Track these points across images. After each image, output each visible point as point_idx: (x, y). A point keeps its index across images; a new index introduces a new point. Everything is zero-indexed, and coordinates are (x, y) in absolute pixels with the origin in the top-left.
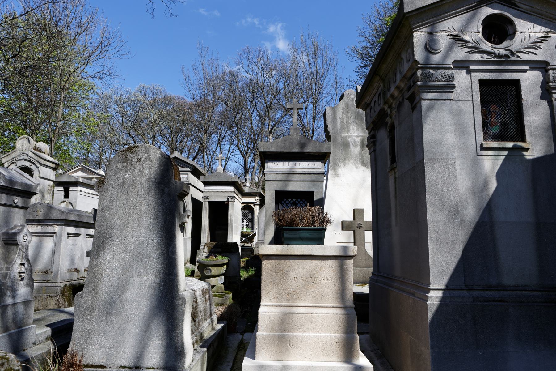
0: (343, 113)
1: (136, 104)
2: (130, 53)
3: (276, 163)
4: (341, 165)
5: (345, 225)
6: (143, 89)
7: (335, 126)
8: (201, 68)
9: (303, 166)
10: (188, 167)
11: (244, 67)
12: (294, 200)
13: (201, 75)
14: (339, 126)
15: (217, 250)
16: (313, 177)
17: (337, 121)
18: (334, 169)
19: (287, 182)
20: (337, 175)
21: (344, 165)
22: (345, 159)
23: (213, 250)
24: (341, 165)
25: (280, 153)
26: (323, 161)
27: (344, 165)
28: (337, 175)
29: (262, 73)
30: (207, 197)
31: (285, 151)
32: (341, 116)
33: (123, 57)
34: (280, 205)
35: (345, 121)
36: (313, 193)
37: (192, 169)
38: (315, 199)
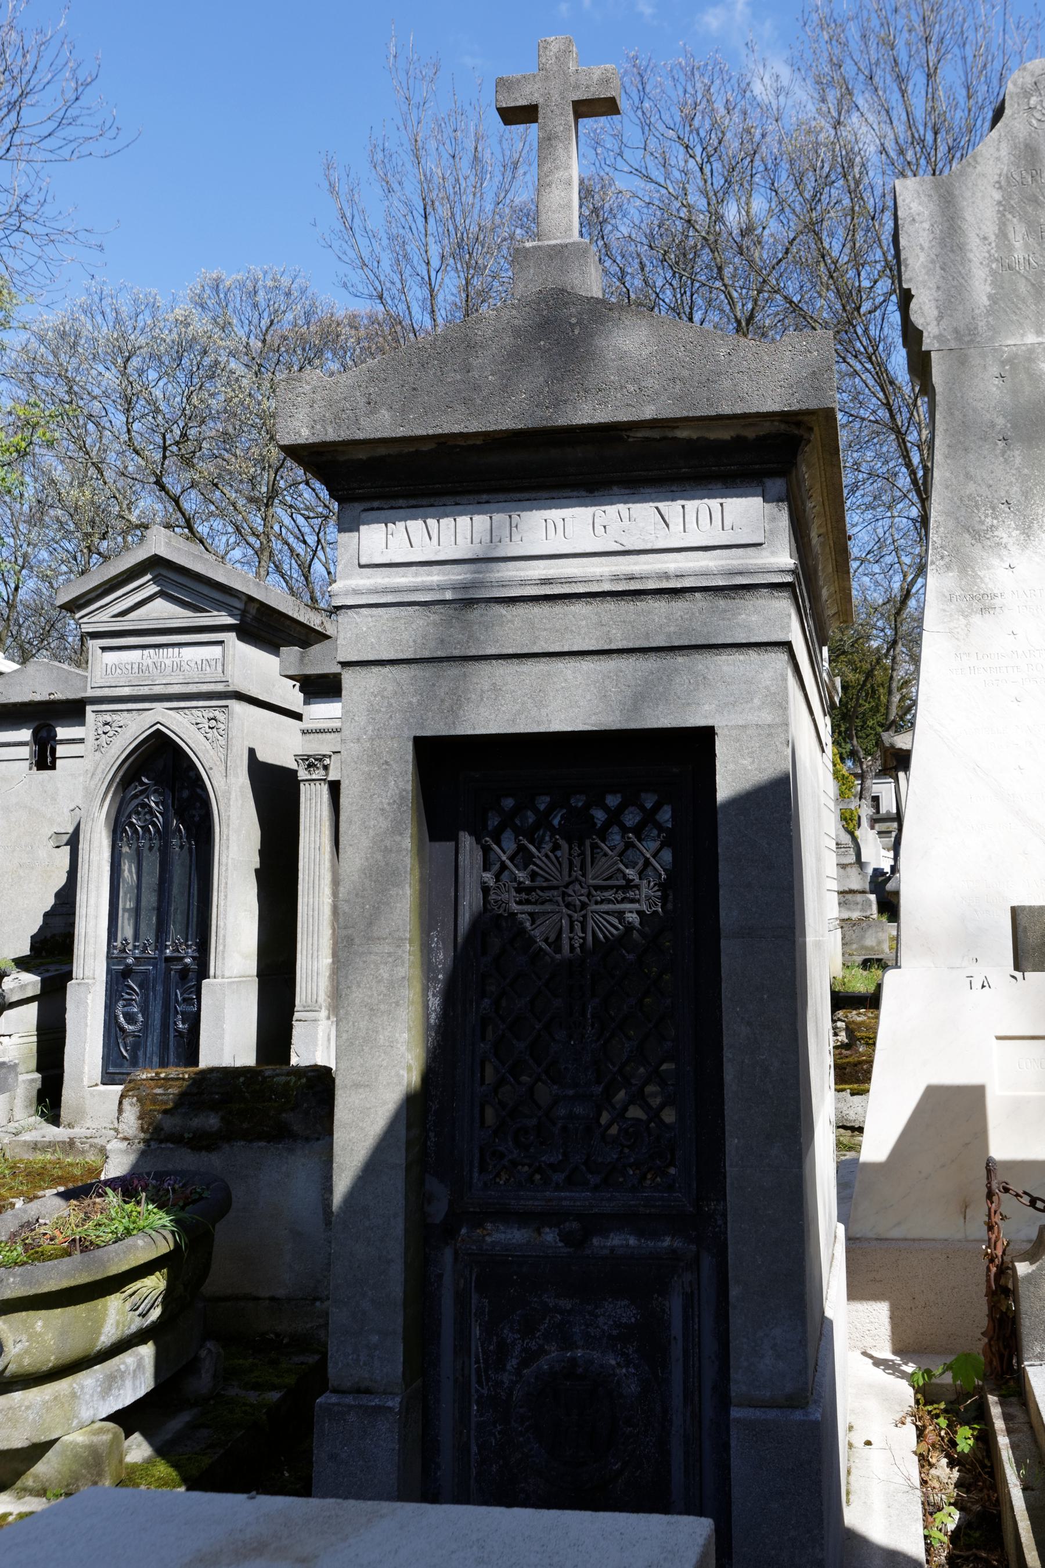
0: (1005, 208)
1: (187, 355)
2: (113, 132)
3: (416, 526)
4: (1007, 533)
5: (1032, 938)
6: (217, 289)
7: (954, 293)
8: (408, 159)
9: (568, 537)
10: (220, 606)
11: (627, 154)
12: (578, 801)
13: (412, 191)
14: (981, 288)
15: (196, 1122)
16: (661, 620)
17: (965, 261)
18: (963, 564)
19: (453, 671)
20: (983, 603)
21: (1027, 531)
22: (1026, 494)
23: (170, 1124)
24: (1007, 533)
25: (444, 443)
26: (777, 485)
27: (1027, 531)
28: (983, 603)
29: (707, 169)
30: (321, 758)
31: (474, 426)
32: (990, 229)
33: (85, 149)
34: (467, 841)
35: (1019, 254)
36: (700, 742)
37: (243, 615)
38: (725, 788)
